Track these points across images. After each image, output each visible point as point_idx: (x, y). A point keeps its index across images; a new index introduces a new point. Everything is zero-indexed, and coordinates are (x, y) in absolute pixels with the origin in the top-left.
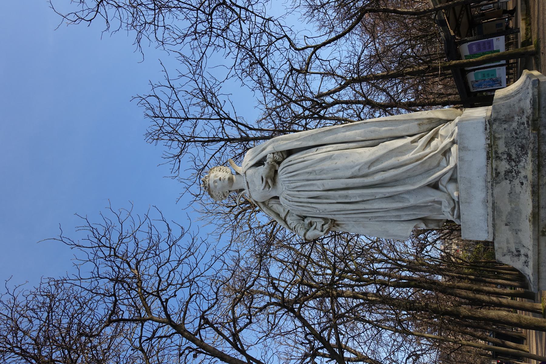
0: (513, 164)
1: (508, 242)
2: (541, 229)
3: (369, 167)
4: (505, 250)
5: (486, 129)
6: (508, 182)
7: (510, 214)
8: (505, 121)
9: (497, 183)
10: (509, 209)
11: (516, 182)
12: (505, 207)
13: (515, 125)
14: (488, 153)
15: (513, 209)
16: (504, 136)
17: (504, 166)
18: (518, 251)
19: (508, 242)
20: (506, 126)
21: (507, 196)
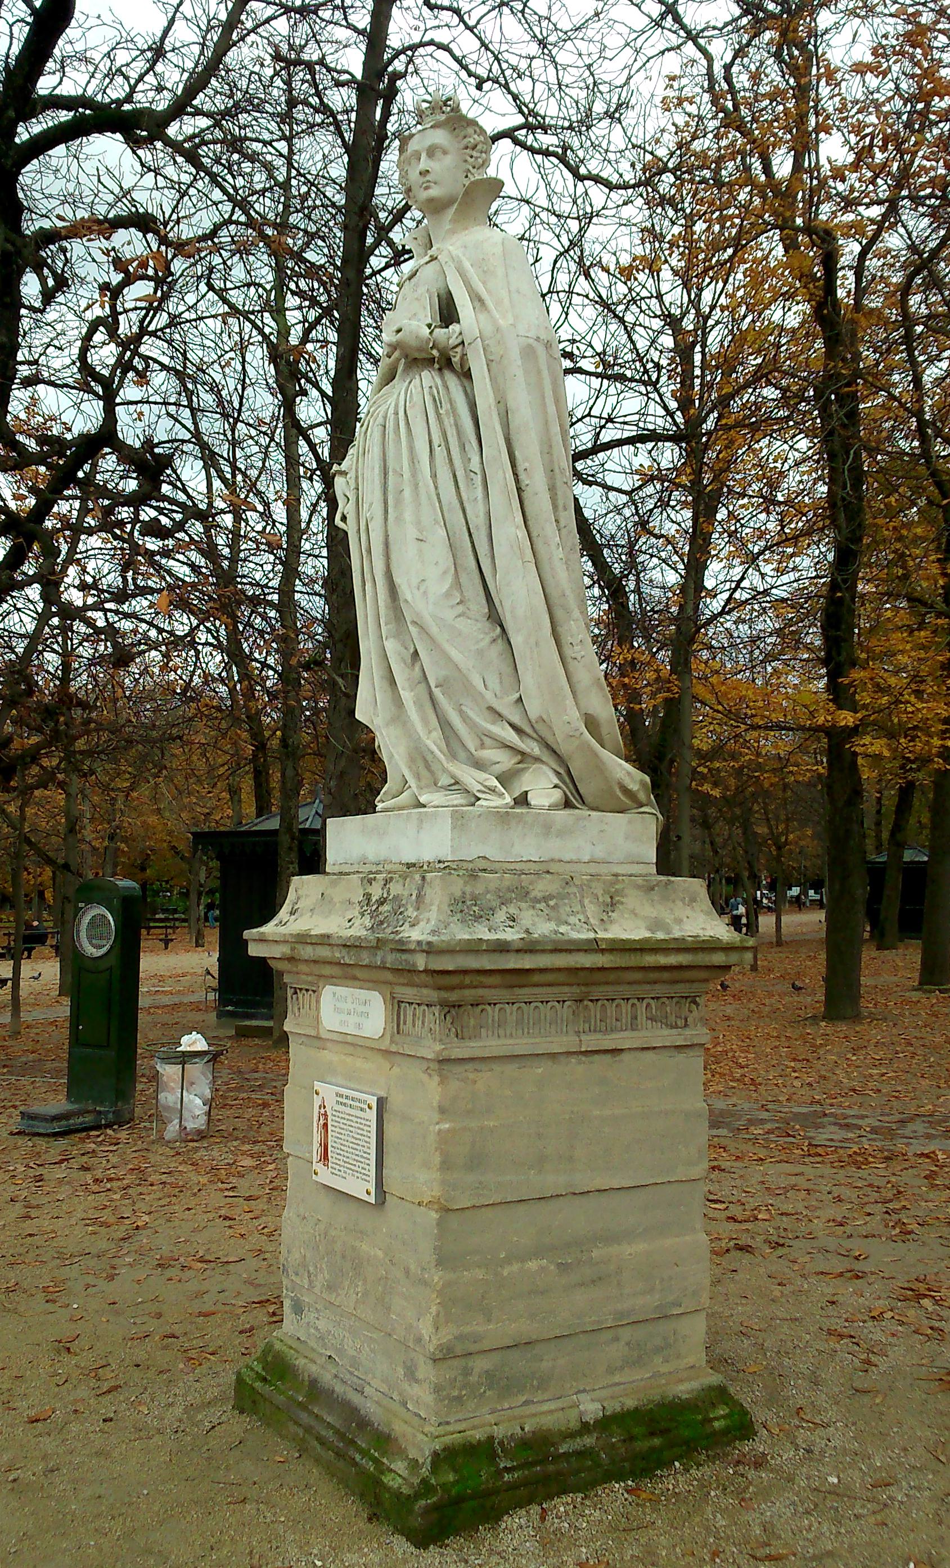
3: (414, 623)
14: (414, 865)
20: (414, 897)
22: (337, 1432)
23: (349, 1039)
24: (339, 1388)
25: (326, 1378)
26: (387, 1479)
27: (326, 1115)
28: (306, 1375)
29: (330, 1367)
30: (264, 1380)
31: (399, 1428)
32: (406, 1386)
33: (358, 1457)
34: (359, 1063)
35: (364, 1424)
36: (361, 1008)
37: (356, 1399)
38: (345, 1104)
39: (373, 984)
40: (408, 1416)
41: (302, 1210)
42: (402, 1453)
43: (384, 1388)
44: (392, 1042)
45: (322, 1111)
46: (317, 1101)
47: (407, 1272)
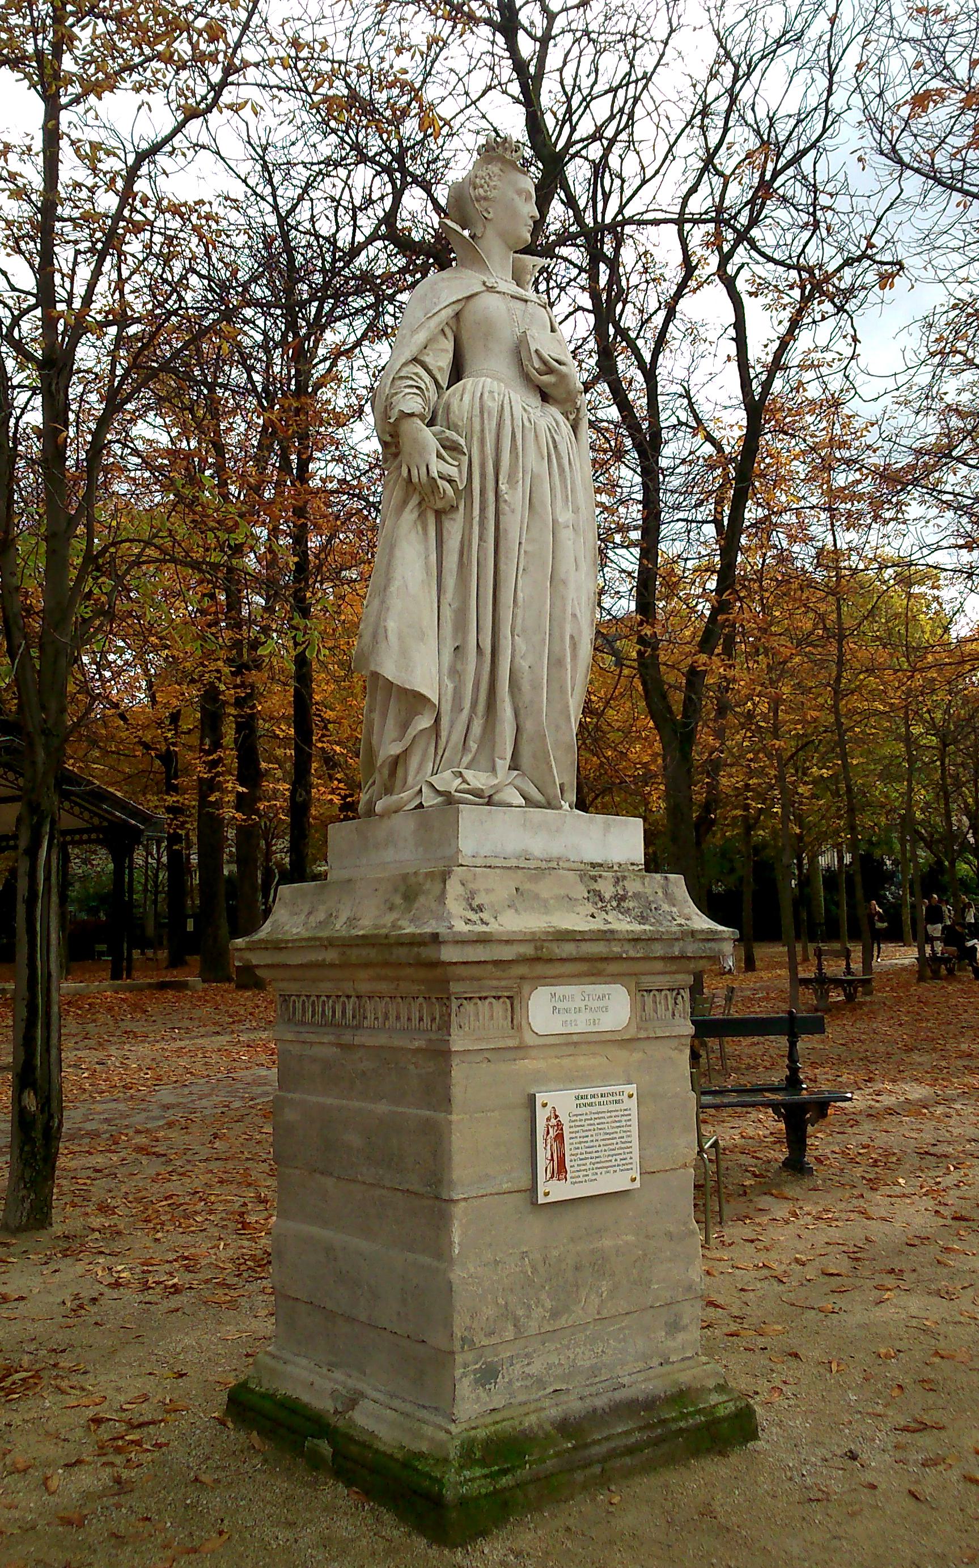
0: (615, 904)
1: (488, 891)
2: (546, 944)
4: (471, 886)
5: (632, 864)
6: (586, 895)
7: (537, 897)
8: (666, 894)
9: (581, 876)
10: (544, 895)
11: (590, 909)
12: (546, 889)
13: (666, 907)
14: (601, 865)
15: (546, 901)
16: (649, 891)
17: (608, 890)
18: (480, 908)
19: (488, 891)
20: (660, 894)
21: (563, 892)
22: (640, 1429)
23: (575, 1038)
24: (600, 1402)
25: (574, 1406)
26: (721, 1412)
27: (559, 1125)
28: (548, 1427)
29: (564, 1398)
30: (504, 1472)
31: (685, 1378)
32: (670, 1343)
33: (682, 1424)
34: (582, 1061)
35: (650, 1404)
36: (601, 1004)
37: (619, 1395)
38: (591, 1105)
39: (614, 978)
40: (682, 1365)
41: (488, 1256)
42: (704, 1390)
43: (641, 1365)
44: (639, 1028)
45: (553, 1121)
46: (542, 1116)
47: (670, 1236)
